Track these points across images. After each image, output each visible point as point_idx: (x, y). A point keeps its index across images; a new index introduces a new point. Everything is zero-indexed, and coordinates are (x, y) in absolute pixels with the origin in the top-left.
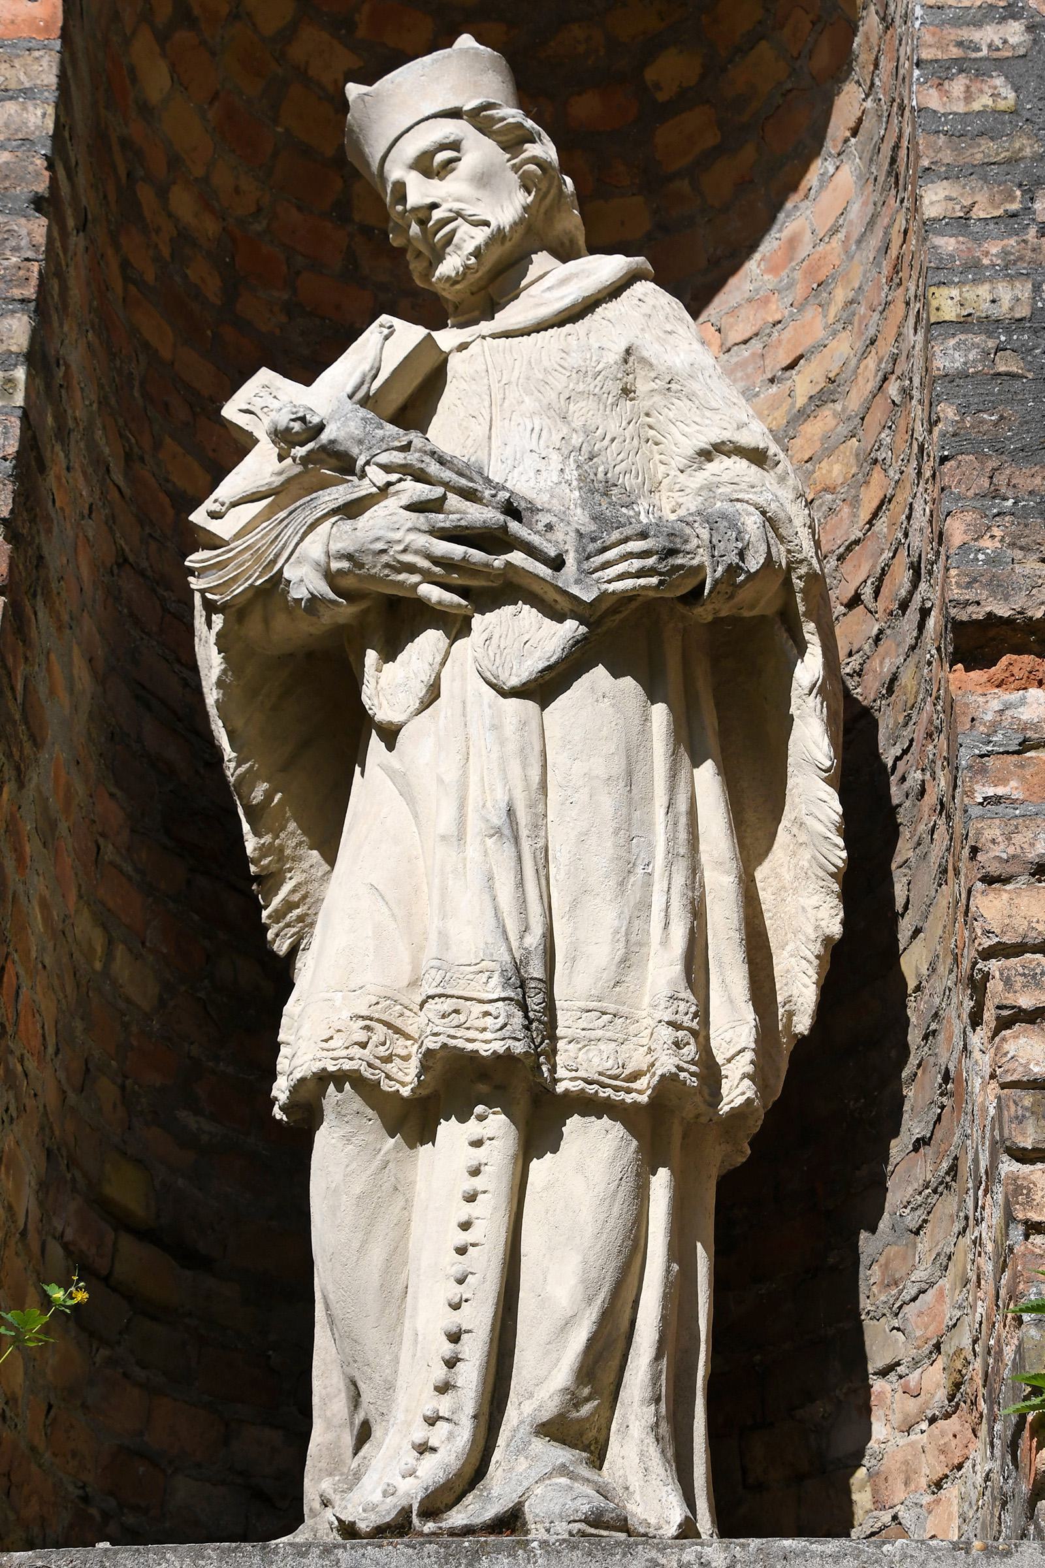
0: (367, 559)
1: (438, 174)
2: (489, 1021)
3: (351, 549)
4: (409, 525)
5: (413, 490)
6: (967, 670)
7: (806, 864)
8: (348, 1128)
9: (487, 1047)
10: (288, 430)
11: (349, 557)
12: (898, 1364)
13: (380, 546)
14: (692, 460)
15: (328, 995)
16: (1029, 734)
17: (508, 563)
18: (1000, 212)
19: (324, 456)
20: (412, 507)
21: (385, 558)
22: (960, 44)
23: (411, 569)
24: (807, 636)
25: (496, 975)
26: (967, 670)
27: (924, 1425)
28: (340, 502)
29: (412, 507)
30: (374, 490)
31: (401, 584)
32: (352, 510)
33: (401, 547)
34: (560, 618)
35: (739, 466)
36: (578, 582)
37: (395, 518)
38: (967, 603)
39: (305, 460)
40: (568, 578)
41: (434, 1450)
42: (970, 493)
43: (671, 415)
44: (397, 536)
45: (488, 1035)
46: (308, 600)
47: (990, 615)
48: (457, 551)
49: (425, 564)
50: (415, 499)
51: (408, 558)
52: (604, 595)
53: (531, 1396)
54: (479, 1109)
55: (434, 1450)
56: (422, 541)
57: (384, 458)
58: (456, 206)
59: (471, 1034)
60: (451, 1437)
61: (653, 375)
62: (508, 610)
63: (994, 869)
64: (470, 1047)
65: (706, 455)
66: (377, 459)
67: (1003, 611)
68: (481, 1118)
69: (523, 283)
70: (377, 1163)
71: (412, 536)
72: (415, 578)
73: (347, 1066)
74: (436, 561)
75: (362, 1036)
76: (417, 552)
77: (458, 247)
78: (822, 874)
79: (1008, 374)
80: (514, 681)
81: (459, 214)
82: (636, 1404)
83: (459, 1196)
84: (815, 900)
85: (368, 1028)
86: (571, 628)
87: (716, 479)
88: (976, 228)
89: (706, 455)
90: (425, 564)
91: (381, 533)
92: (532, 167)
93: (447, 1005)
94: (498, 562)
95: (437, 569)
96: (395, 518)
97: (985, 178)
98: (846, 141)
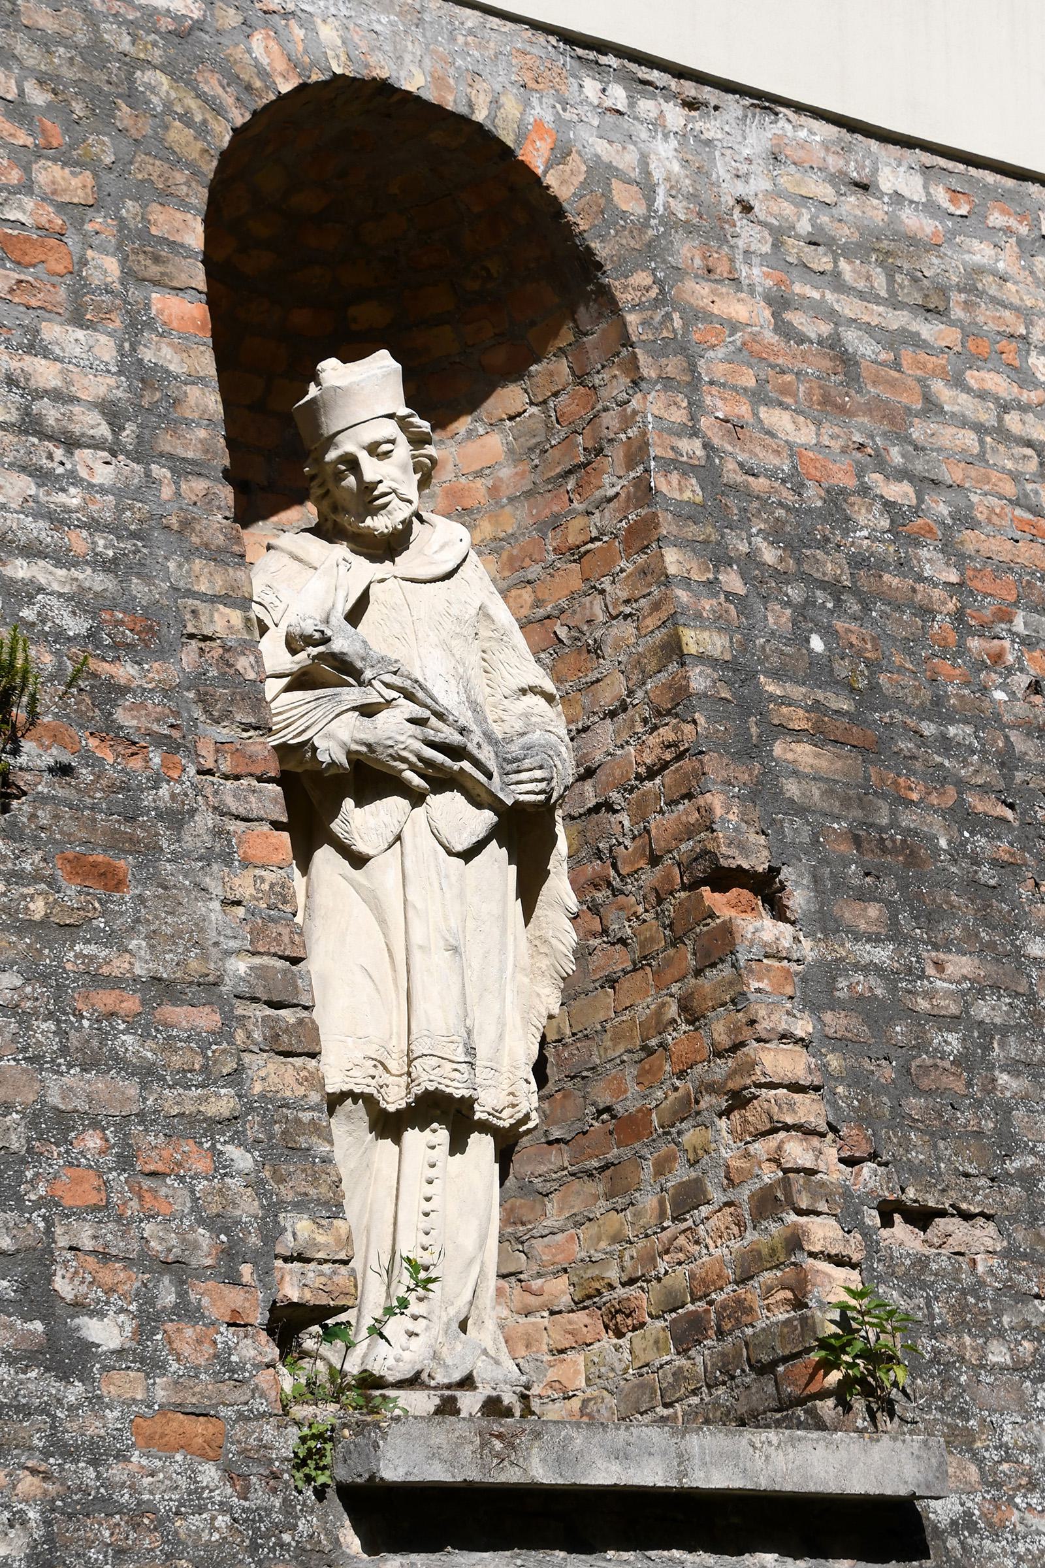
0: (379, 749)
1: (378, 455)
2: (456, 1075)
3: (372, 741)
4: (410, 733)
5: (409, 709)
6: (713, 891)
7: (544, 967)
8: (352, 1127)
9: (458, 1091)
10: (311, 636)
11: (369, 745)
12: (521, 1273)
13: (390, 743)
14: (515, 693)
15: (343, 1038)
16: (767, 949)
17: (461, 768)
18: (704, 579)
19: (330, 658)
20: (411, 721)
21: (391, 751)
22: (672, 448)
23: (404, 760)
24: (557, 818)
25: (461, 1045)
26: (713, 891)
27: (546, 1314)
28: (358, 703)
29: (411, 721)
30: (382, 700)
31: (393, 767)
32: (368, 711)
33: (403, 746)
34: (479, 806)
35: (541, 701)
36: (502, 789)
37: (401, 726)
38: (729, 857)
39: (315, 657)
40: (495, 785)
41: (417, 1335)
42: (719, 780)
43: (501, 657)
44: (402, 738)
45: (456, 1084)
46: (329, 764)
47: (739, 867)
48: (439, 757)
49: (414, 759)
50: (414, 716)
51: (405, 754)
52: (516, 802)
53: (452, 1304)
54: (435, 1125)
55: (417, 1335)
56: (418, 746)
57: (388, 678)
58: (394, 486)
59: (448, 1082)
60: (427, 1328)
61: (493, 627)
62: (448, 794)
63: (764, 1035)
64: (448, 1090)
65: (524, 692)
66: (381, 677)
67: (746, 866)
68: (434, 1131)
69: (412, 539)
70: (363, 1149)
71: (410, 741)
72: (404, 766)
73: (367, 1090)
74: (421, 759)
75: (372, 1072)
76: (411, 751)
77: (390, 513)
78: (556, 976)
79: (726, 699)
80: (459, 848)
81: (394, 491)
82: (488, 1310)
83: (424, 1180)
84: (547, 991)
85: (375, 1066)
86: (488, 818)
87: (530, 710)
88: (695, 586)
89: (524, 692)
90: (414, 759)
91: (393, 735)
92: (427, 461)
93: (434, 1061)
94: (456, 766)
95: (420, 764)
96: (401, 726)
97: (693, 550)
98: (502, 420)
